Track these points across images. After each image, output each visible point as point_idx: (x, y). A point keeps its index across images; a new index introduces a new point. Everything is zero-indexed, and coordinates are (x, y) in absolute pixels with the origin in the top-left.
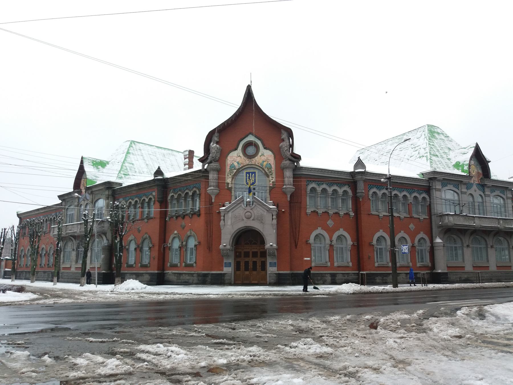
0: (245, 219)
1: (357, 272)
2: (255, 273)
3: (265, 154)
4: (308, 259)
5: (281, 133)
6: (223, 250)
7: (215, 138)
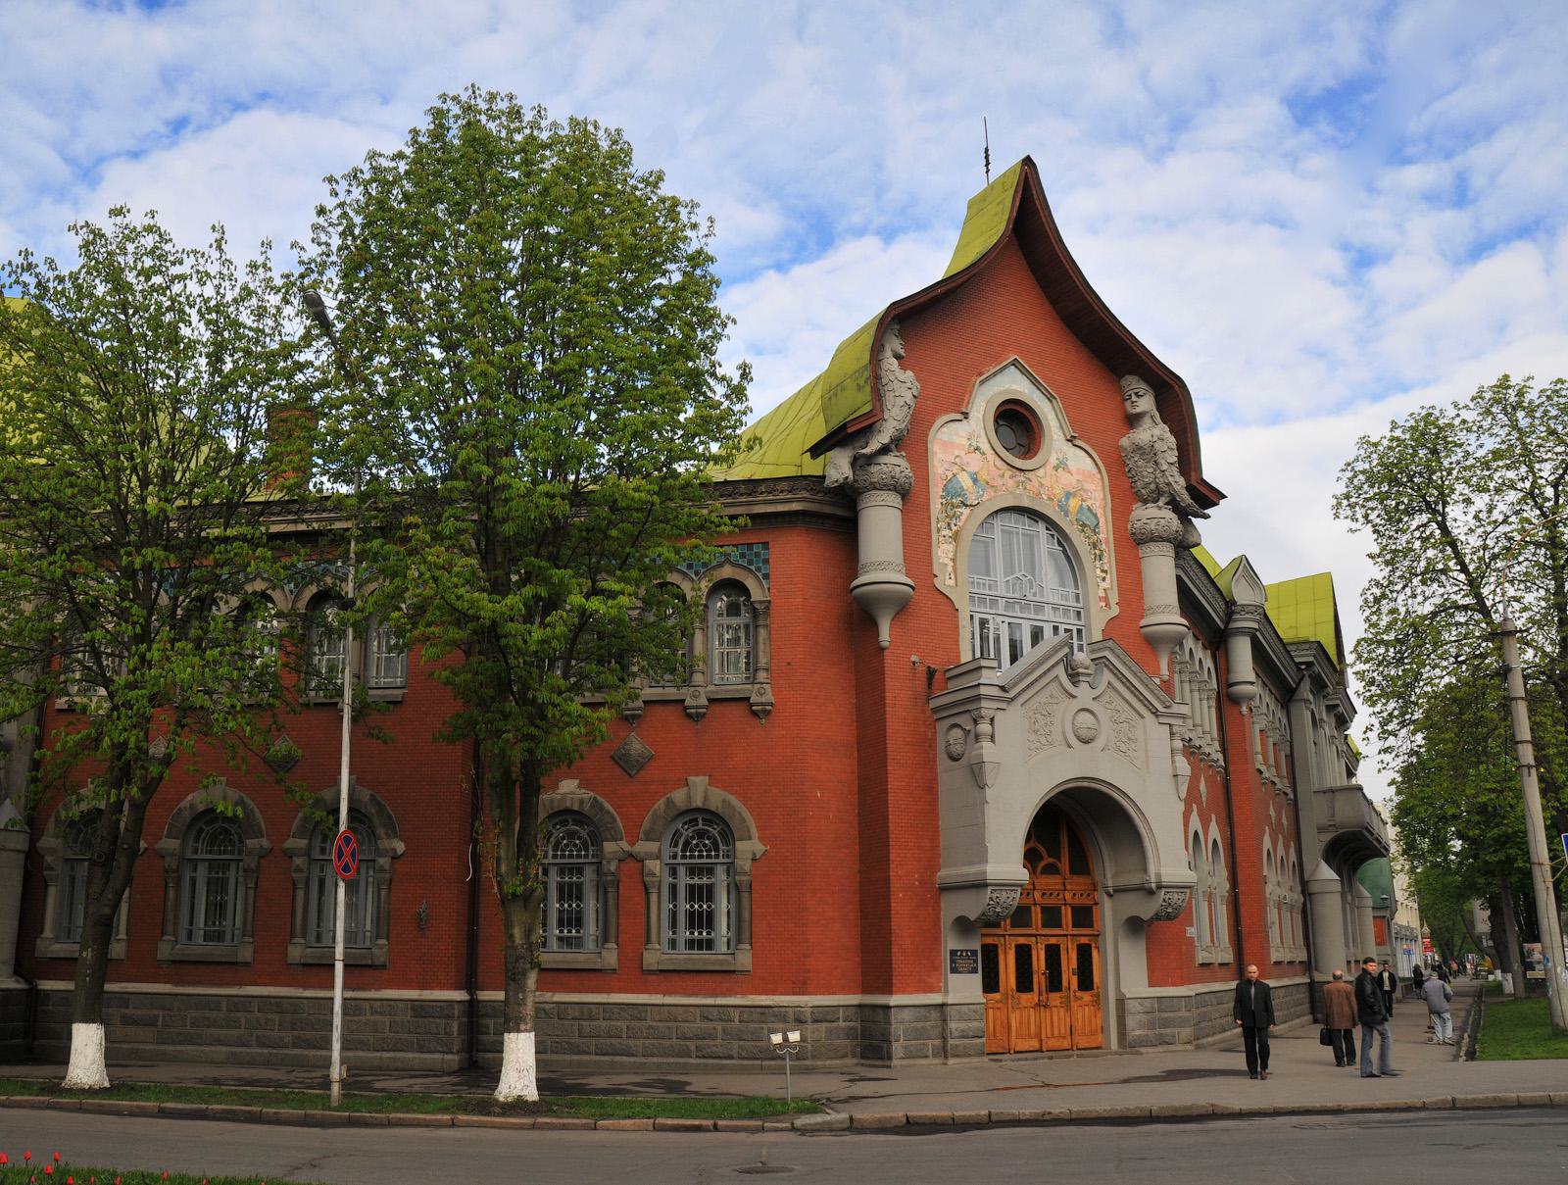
0: (1073, 740)
2: (1055, 998)
3: (1071, 465)
5: (1120, 390)
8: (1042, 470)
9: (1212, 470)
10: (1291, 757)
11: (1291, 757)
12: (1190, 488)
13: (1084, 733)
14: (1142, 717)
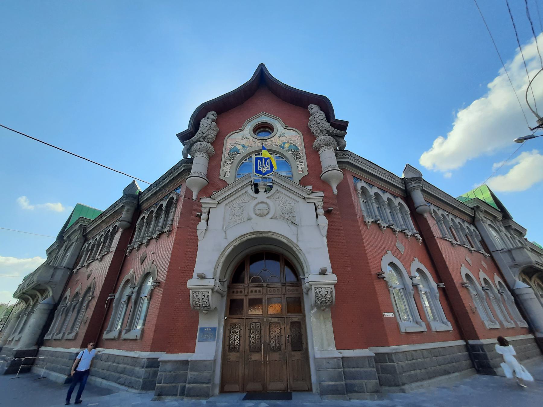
0: (253, 216)
1: (461, 343)
4: (391, 315)
6: (198, 290)
7: (212, 115)
8: (273, 139)
9: (339, 116)
10: (483, 242)
11: (483, 242)
12: (332, 125)
13: (258, 212)
14: (298, 202)
